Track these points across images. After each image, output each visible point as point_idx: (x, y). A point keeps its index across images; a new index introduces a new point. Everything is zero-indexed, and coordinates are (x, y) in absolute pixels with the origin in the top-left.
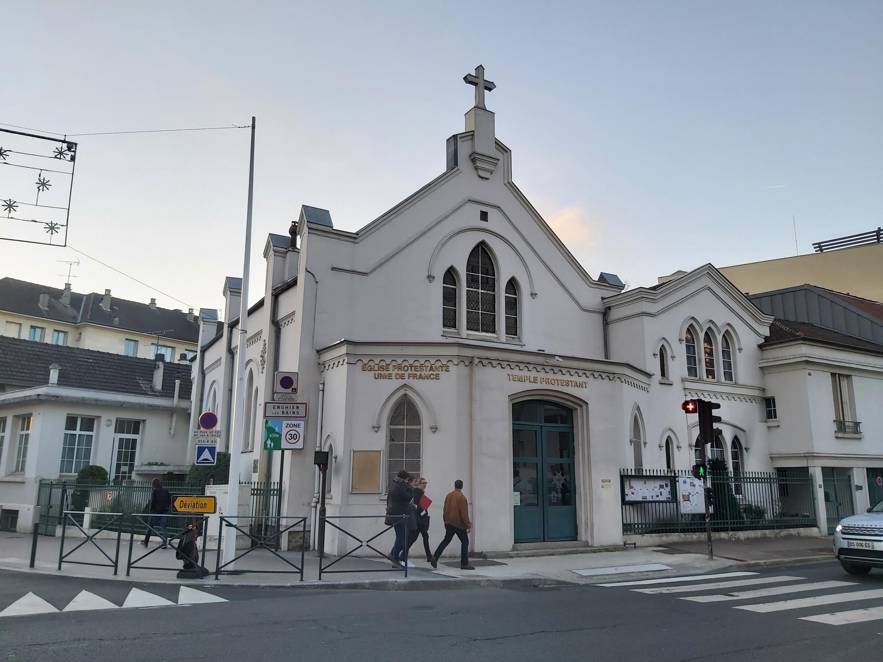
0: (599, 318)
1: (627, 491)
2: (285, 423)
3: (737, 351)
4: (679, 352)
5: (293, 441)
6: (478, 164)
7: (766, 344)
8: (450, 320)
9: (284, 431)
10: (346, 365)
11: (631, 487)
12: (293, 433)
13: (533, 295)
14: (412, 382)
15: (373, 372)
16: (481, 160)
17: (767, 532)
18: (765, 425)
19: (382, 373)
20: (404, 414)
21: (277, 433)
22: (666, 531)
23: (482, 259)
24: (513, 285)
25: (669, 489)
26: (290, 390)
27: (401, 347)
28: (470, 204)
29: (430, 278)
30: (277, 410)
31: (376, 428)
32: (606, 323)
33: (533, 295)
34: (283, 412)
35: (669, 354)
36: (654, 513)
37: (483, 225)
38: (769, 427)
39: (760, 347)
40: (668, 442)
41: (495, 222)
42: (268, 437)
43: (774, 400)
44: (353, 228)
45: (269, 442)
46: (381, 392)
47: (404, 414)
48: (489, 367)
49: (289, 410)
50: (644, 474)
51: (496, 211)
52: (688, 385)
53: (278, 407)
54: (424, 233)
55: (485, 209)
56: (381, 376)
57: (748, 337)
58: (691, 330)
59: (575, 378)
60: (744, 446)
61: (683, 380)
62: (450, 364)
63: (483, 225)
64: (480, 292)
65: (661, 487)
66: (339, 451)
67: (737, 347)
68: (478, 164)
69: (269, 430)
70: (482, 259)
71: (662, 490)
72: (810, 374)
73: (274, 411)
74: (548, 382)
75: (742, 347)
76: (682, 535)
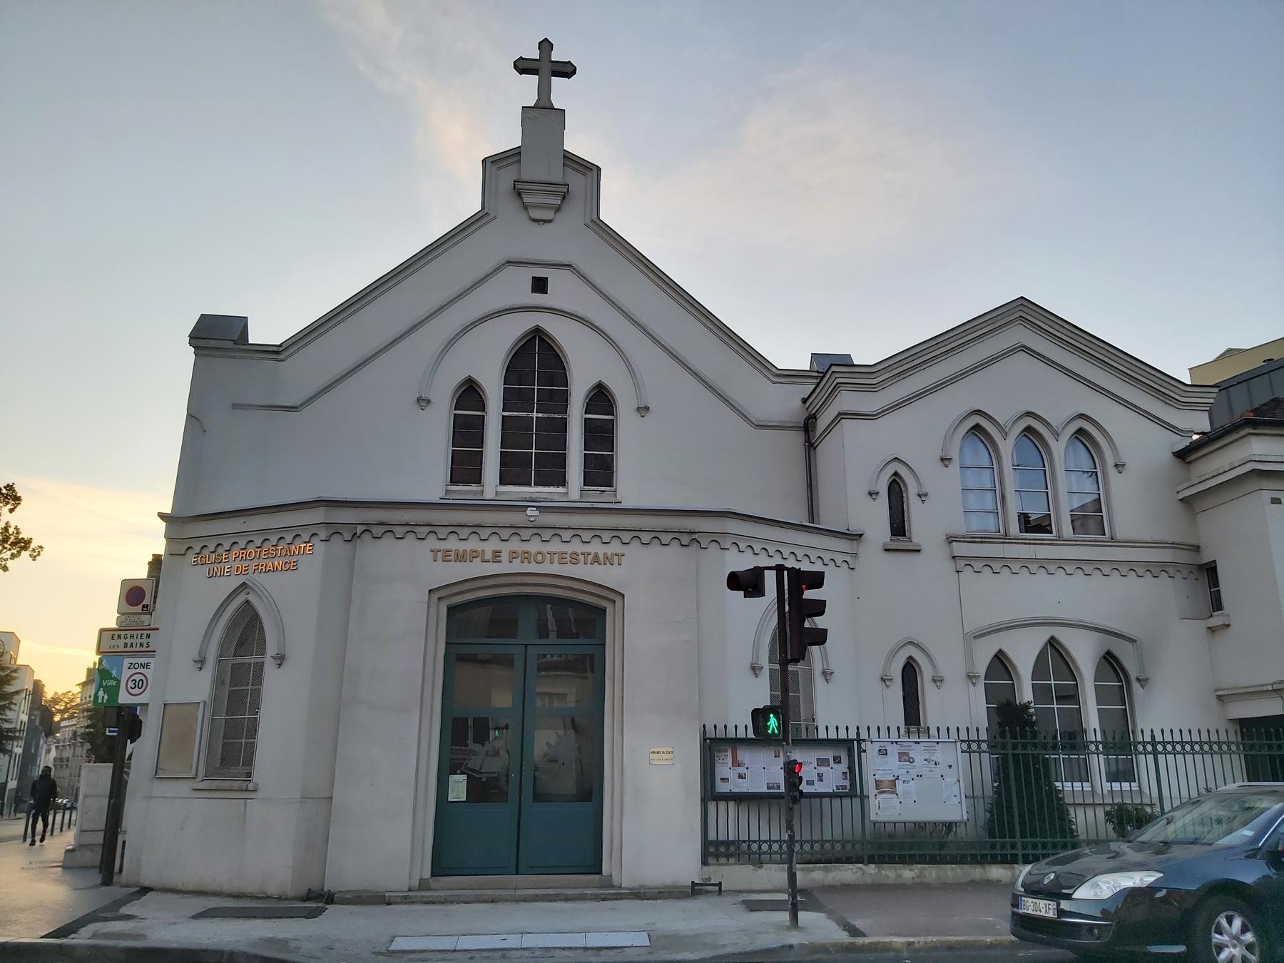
0: (799, 437)
2: (127, 661)
3: (1112, 472)
5: (137, 691)
9: (126, 673)
11: (736, 763)
12: (138, 677)
15: (206, 568)
16: (530, 191)
18: (1201, 625)
21: (115, 679)
22: (892, 860)
23: (536, 362)
24: (601, 398)
25: (843, 767)
26: (139, 609)
27: (242, 519)
28: (511, 269)
30: (116, 642)
32: (810, 447)
33: (643, 410)
34: (126, 645)
35: (912, 490)
38: (1212, 630)
40: (910, 673)
41: (562, 291)
42: (101, 686)
44: (276, 336)
45: (101, 693)
49: (134, 641)
50: (822, 735)
51: (565, 273)
53: (132, 636)
54: (413, 328)
55: (540, 273)
59: (596, 548)
60: (1133, 672)
64: (535, 417)
65: (822, 762)
67: (1110, 461)
70: (536, 362)
71: (823, 770)
72: (1276, 501)
73: (114, 642)
75: (1125, 458)
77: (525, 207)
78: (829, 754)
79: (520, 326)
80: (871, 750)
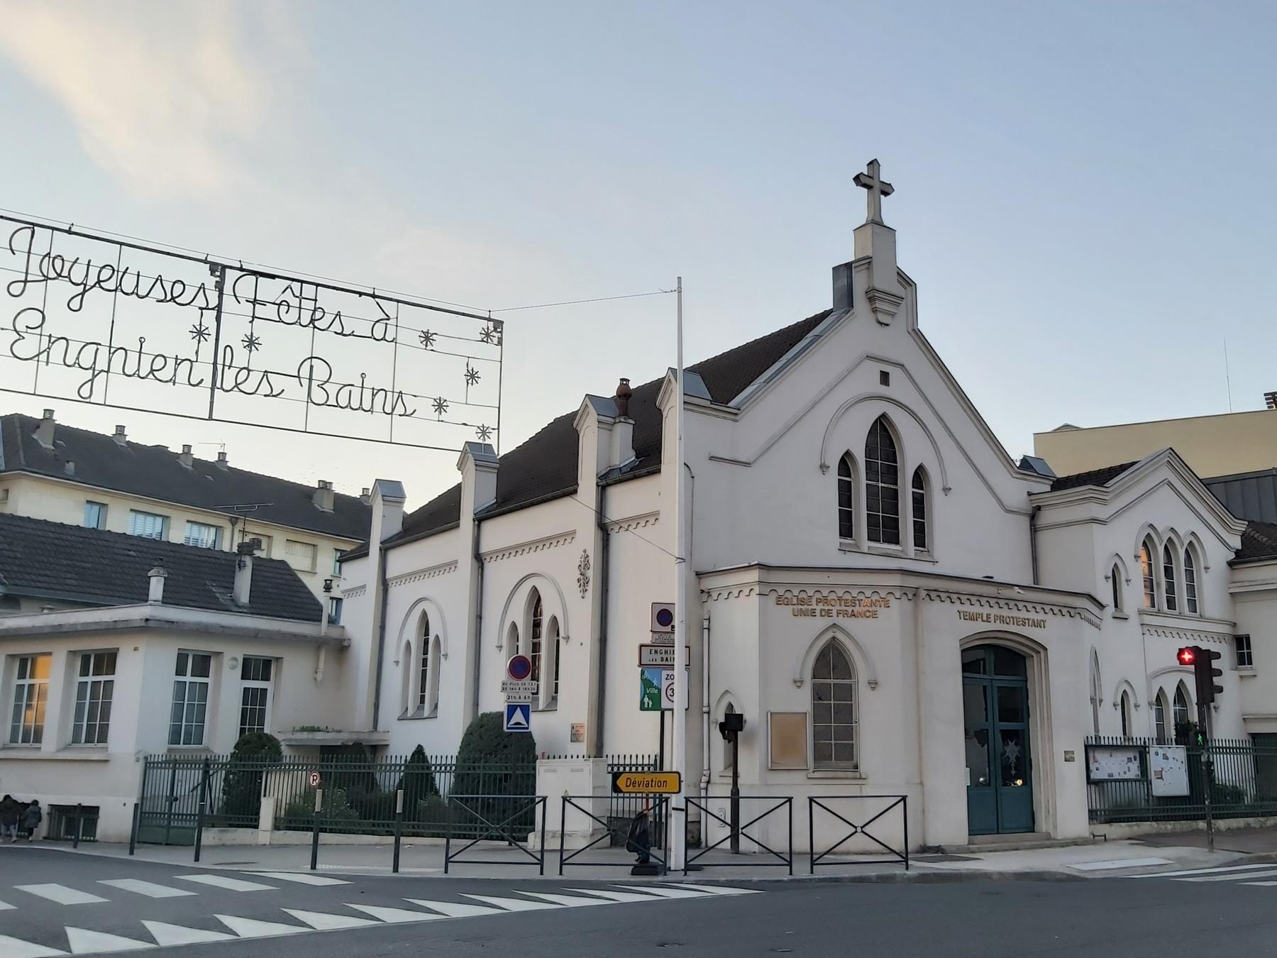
1: (1092, 767)
4: (1135, 571)
6: (878, 305)
7: (1240, 559)
8: (846, 529)
10: (754, 599)
13: (946, 490)
14: (841, 621)
17: (1251, 820)
19: (803, 608)
20: (832, 664)
23: (883, 437)
24: (920, 477)
26: (668, 629)
29: (824, 467)
30: (653, 656)
31: (798, 683)
33: (946, 490)
36: (1120, 795)
37: (883, 390)
39: (1231, 564)
43: (1248, 638)
45: (646, 700)
46: (803, 636)
47: (832, 664)
52: (1148, 619)
55: (886, 368)
56: (803, 613)
57: (1216, 551)
58: (1148, 544)
61: (1141, 613)
62: (891, 598)
63: (883, 390)
66: (752, 713)
68: (878, 305)
69: (646, 683)
70: (883, 437)
74: (1002, 619)
76: (1154, 823)
77: (875, 311)
78: (1131, 755)
79: (871, 413)
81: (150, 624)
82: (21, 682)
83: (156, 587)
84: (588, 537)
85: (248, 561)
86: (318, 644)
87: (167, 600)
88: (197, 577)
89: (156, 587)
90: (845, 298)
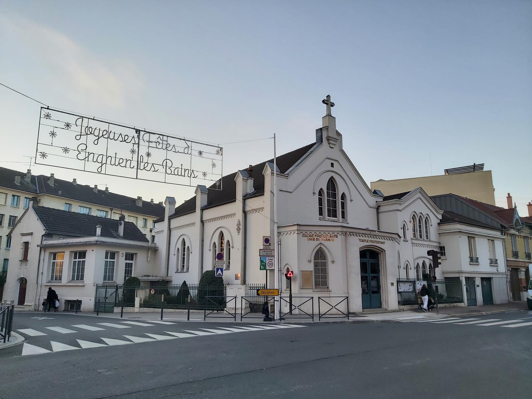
2: (267, 258)
4: (410, 226)
6: (330, 142)
7: (442, 222)
8: (321, 213)
9: (267, 262)
10: (296, 235)
13: (351, 200)
14: (323, 242)
19: (311, 238)
20: (320, 256)
23: (332, 184)
24: (343, 196)
26: (268, 244)
29: (314, 193)
31: (310, 261)
32: (378, 213)
33: (351, 200)
36: (406, 296)
37: (332, 169)
39: (439, 224)
41: (337, 168)
43: (444, 247)
46: (311, 246)
47: (320, 256)
48: (352, 236)
52: (414, 241)
55: (333, 162)
56: (311, 239)
57: (434, 221)
58: (414, 218)
61: (412, 239)
62: (338, 235)
63: (332, 169)
66: (296, 272)
68: (330, 142)
69: (262, 261)
70: (332, 184)
74: (372, 242)
77: (329, 143)
79: (328, 176)
80: (417, 283)
81: (98, 242)
82: (75, 260)
83: (99, 231)
84: (240, 216)
85: (123, 222)
86: (148, 249)
87: (102, 235)
88: (110, 228)
89: (99, 231)
90: (320, 139)
